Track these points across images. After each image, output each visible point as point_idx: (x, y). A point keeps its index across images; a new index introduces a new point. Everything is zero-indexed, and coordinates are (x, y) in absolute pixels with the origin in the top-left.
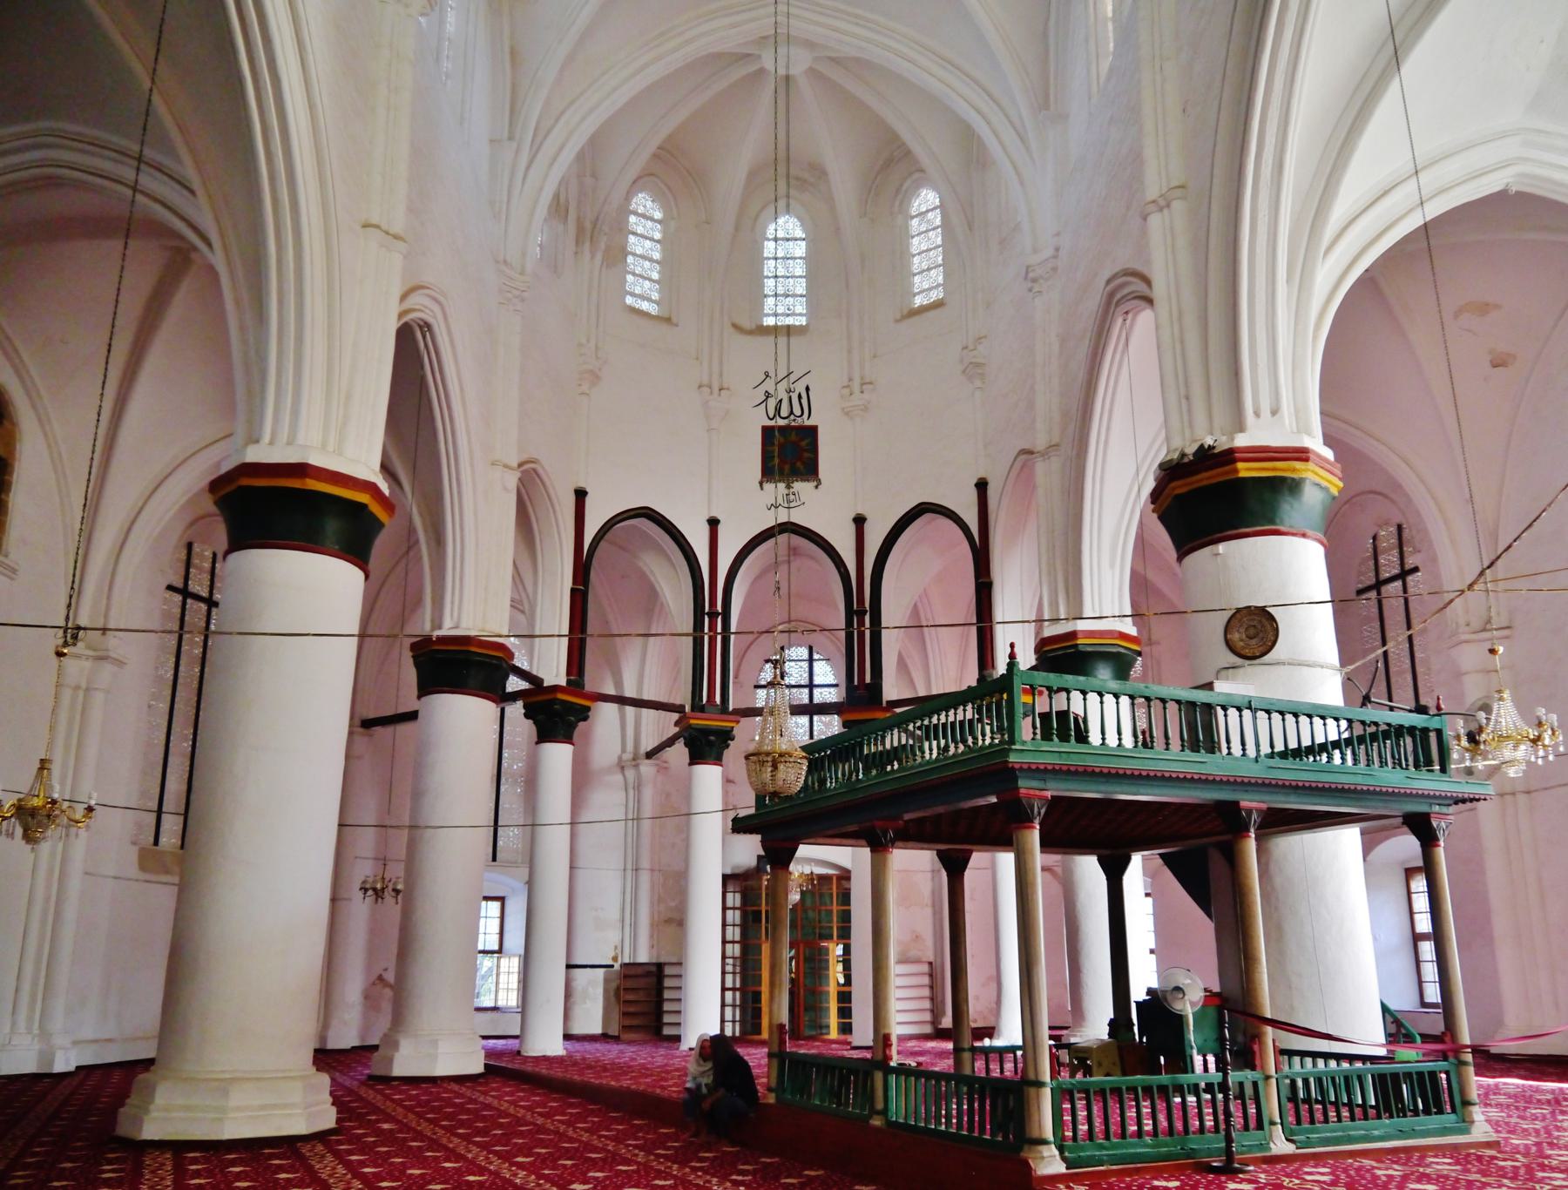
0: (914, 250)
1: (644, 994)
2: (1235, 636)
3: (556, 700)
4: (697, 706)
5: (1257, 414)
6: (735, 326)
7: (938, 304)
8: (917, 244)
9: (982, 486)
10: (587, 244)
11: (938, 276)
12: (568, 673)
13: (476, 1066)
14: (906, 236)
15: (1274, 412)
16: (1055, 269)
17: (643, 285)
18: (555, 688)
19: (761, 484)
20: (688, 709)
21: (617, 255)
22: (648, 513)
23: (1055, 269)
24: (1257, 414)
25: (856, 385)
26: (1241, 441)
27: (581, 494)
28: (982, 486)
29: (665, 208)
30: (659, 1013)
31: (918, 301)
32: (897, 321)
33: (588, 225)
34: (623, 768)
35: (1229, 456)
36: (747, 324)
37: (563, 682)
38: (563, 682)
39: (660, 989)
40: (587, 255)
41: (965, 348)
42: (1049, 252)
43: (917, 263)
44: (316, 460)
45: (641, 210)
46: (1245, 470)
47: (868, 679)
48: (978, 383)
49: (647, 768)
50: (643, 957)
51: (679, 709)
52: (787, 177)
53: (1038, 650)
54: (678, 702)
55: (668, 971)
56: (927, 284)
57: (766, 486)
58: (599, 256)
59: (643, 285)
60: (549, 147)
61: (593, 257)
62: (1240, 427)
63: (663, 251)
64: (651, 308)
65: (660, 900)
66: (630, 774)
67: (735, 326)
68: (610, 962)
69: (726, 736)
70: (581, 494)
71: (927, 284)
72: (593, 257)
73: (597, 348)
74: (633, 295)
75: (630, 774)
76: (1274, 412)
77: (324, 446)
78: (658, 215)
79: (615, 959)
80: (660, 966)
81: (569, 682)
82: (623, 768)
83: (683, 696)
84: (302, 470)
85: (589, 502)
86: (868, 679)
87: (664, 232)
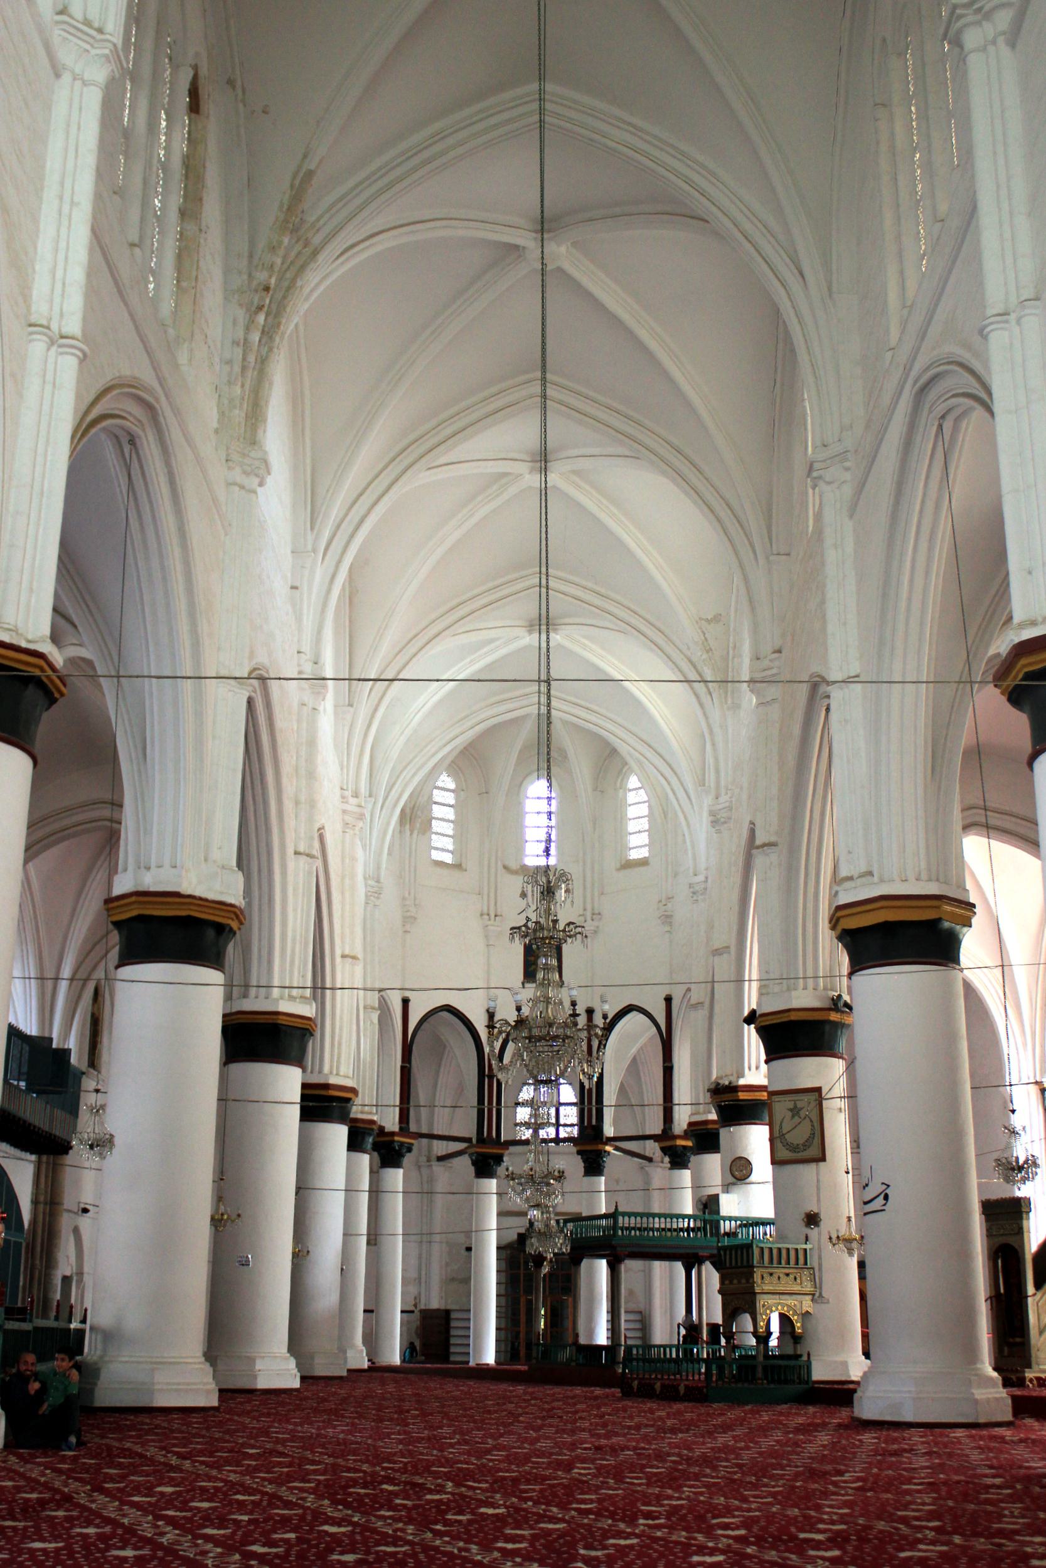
0: (630, 815)
1: (436, 1333)
2: (743, 1162)
3: (393, 1141)
4: (481, 1140)
5: (750, 1069)
6: (505, 867)
7: (643, 862)
8: (632, 812)
9: (668, 1000)
10: (408, 826)
11: (644, 838)
12: (401, 1121)
13: (365, 1365)
14: (623, 805)
15: (757, 1068)
16: (705, 889)
17: (442, 843)
18: (393, 1134)
19: (523, 983)
20: (474, 1141)
21: (427, 827)
22: (449, 1009)
23: (705, 889)
24: (750, 1069)
25: (589, 918)
26: (742, 1082)
27: (406, 1002)
28: (668, 1000)
29: (456, 779)
30: (447, 1345)
31: (634, 855)
32: (618, 870)
33: (408, 811)
34: (419, 1167)
35: (733, 1089)
36: (514, 866)
37: (396, 1129)
38: (396, 1129)
39: (447, 1328)
40: (408, 833)
41: (660, 901)
42: (701, 878)
43: (632, 826)
44: (333, 1080)
45: (439, 784)
46: (742, 1096)
47: (594, 1122)
48: (667, 928)
49: (438, 1168)
50: (435, 1304)
51: (468, 1140)
52: (545, 756)
53: (690, 1124)
54: (467, 1136)
55: (453, 1315)
56: (638, 846)
57: (527, 985)
58: (416, 832)
59: (442, 843)
60: (394, 794)
61: (411, 834)
62: (742, 1076)
63: (456, 813)
64: (448, 858)
65: (447, 1264)
66: (425, 1171)
67: (505, 867)
68: (412, 1308)
69: (499, 1159)
70: (406, 1002)
71: (638, 846)
72: (411, 834)
73: (415, 899)
74: (437, 849)
75: (425, 1171)
76: (757, 1068)
77: (331, 1073)
78: (452, 786)
79: (415, 1306)
80: (447, 1312)
81: (401, 1129)
82: (419, 1167)
83: (470, 1131)
84: (326, 1086)
85: (411, 1004)
86: (594, 1122)
87: (457, 799)
